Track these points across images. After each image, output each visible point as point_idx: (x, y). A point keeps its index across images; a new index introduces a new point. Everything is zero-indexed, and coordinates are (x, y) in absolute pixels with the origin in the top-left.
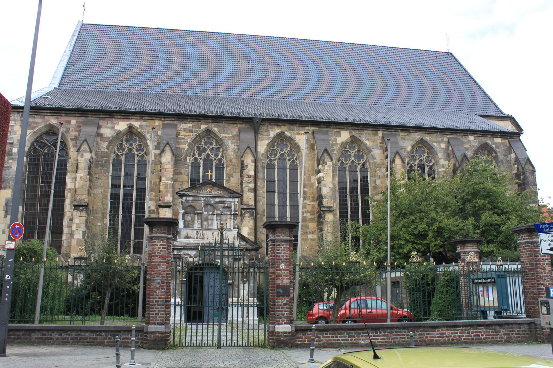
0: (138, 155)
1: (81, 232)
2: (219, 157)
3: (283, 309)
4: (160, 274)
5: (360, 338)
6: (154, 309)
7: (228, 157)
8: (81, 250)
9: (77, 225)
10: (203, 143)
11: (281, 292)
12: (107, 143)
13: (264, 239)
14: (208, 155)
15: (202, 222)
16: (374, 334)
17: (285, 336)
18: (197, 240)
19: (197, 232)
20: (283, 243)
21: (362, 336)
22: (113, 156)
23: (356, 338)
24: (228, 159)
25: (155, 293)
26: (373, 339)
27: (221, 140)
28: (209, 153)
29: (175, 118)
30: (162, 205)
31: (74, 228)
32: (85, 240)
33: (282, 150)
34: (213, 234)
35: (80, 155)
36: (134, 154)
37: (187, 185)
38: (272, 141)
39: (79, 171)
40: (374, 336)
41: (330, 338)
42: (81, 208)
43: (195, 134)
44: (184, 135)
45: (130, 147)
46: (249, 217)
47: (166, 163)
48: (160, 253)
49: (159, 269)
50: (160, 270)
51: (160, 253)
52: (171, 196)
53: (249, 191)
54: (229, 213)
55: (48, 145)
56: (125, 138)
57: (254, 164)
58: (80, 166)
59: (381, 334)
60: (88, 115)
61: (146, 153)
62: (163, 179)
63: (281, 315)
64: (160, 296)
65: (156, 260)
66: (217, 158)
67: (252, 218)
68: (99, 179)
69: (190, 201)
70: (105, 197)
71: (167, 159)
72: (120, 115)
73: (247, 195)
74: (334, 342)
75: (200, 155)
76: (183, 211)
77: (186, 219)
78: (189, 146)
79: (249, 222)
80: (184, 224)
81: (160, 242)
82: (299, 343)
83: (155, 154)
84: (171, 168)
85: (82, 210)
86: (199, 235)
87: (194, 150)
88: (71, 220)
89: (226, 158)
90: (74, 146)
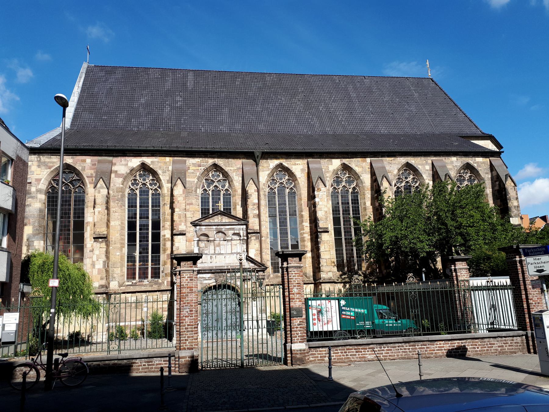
0: (152, 189)
1: (101, 263)
2: (226, 188)
3: (298, 329)
4: (188, 303)
5: (367, 353)
6: (184, 336)
8: (102, 279)
9: (97, 255)
10: (210, 175)
11: (295, 313)
12: (122, 179)
13: (268, 259)
14: (216, 186)
16: (379, 349)
17: (300, 354)
18: (211, 264)
19: (211, 257)
20: (294, 270)
21: (368, 351)
22: (127, 191)
23: (363, 353)
25: (184, 321)
26: (378, 354)
27: (226, 172)
28: (217, 185)
29: (184, 154)
31: (95, 259)
32: (106, 270)
33: (281, 179)
35: (97, 191)
36: (148, 188)
37: (198, 216)
38: (272, 171)
39: (97, 206)
40: (379, 351)
41: (340, 354)
42: (100, 240)
43: (203, 168)
45: (143, 182)
47: (179, 195)
48: (188, 285)
49: (187, 299)
50: (188, 300)
51: (188, 285)
53: (254, 217)
54: (238, 239)
55: (65, 183)
56: (138, 173)
57: (257, 193)
58: (97, 201)
59: (385, 349)
60: (102, 154)
63: (296, 335)
64: (189, 323)
65: (184, 291)
66: (224, 189)
67: (258, 240)
68: (116, 212)
69: (203, 230)
70: (122, 229)
72: (132, 153)
73: (252, 221)
74: (344, 357)
75: (208, 187)
76: (198, 239)
77: (200, 246)
78: (198, 179)
81: (188, 275)
82: (313, 359)
85: (102, 242)
86: (213, 259)
88: (92, 251)
90: (90, 183)
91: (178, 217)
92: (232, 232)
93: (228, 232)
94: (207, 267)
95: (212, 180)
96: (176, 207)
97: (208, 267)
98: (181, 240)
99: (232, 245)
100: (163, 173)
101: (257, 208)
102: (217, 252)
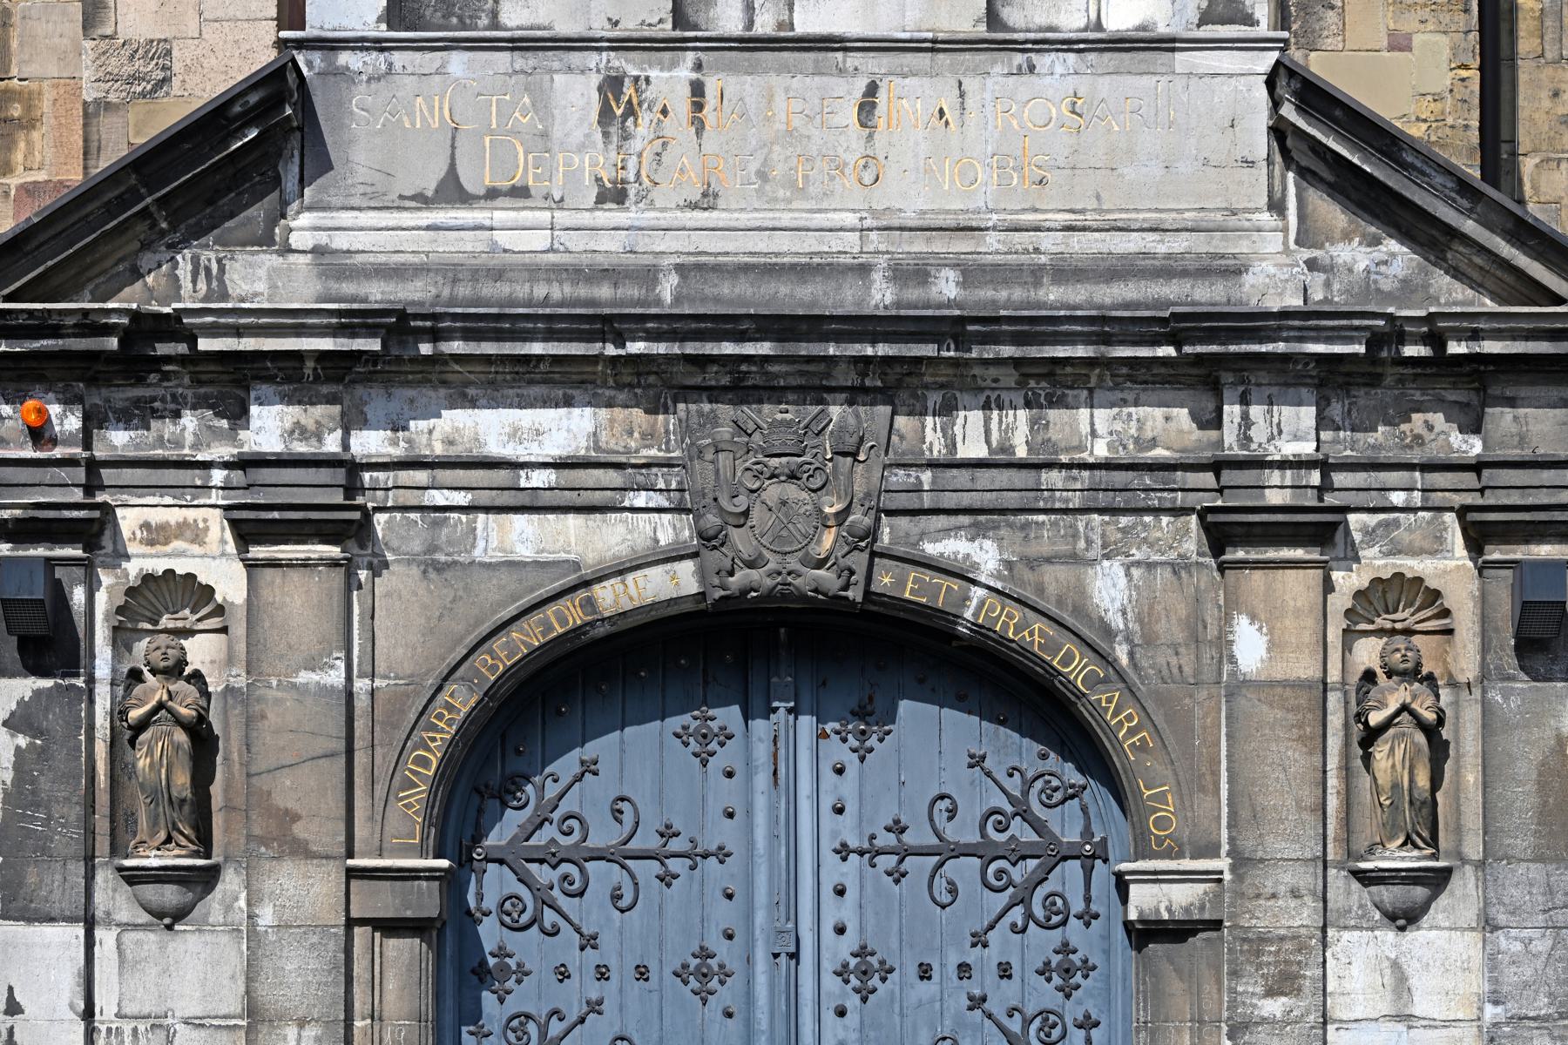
18: (610, 216)
19: (612, 85)
34: (867, 108)
86: (643, 128)
94: (534, 272)
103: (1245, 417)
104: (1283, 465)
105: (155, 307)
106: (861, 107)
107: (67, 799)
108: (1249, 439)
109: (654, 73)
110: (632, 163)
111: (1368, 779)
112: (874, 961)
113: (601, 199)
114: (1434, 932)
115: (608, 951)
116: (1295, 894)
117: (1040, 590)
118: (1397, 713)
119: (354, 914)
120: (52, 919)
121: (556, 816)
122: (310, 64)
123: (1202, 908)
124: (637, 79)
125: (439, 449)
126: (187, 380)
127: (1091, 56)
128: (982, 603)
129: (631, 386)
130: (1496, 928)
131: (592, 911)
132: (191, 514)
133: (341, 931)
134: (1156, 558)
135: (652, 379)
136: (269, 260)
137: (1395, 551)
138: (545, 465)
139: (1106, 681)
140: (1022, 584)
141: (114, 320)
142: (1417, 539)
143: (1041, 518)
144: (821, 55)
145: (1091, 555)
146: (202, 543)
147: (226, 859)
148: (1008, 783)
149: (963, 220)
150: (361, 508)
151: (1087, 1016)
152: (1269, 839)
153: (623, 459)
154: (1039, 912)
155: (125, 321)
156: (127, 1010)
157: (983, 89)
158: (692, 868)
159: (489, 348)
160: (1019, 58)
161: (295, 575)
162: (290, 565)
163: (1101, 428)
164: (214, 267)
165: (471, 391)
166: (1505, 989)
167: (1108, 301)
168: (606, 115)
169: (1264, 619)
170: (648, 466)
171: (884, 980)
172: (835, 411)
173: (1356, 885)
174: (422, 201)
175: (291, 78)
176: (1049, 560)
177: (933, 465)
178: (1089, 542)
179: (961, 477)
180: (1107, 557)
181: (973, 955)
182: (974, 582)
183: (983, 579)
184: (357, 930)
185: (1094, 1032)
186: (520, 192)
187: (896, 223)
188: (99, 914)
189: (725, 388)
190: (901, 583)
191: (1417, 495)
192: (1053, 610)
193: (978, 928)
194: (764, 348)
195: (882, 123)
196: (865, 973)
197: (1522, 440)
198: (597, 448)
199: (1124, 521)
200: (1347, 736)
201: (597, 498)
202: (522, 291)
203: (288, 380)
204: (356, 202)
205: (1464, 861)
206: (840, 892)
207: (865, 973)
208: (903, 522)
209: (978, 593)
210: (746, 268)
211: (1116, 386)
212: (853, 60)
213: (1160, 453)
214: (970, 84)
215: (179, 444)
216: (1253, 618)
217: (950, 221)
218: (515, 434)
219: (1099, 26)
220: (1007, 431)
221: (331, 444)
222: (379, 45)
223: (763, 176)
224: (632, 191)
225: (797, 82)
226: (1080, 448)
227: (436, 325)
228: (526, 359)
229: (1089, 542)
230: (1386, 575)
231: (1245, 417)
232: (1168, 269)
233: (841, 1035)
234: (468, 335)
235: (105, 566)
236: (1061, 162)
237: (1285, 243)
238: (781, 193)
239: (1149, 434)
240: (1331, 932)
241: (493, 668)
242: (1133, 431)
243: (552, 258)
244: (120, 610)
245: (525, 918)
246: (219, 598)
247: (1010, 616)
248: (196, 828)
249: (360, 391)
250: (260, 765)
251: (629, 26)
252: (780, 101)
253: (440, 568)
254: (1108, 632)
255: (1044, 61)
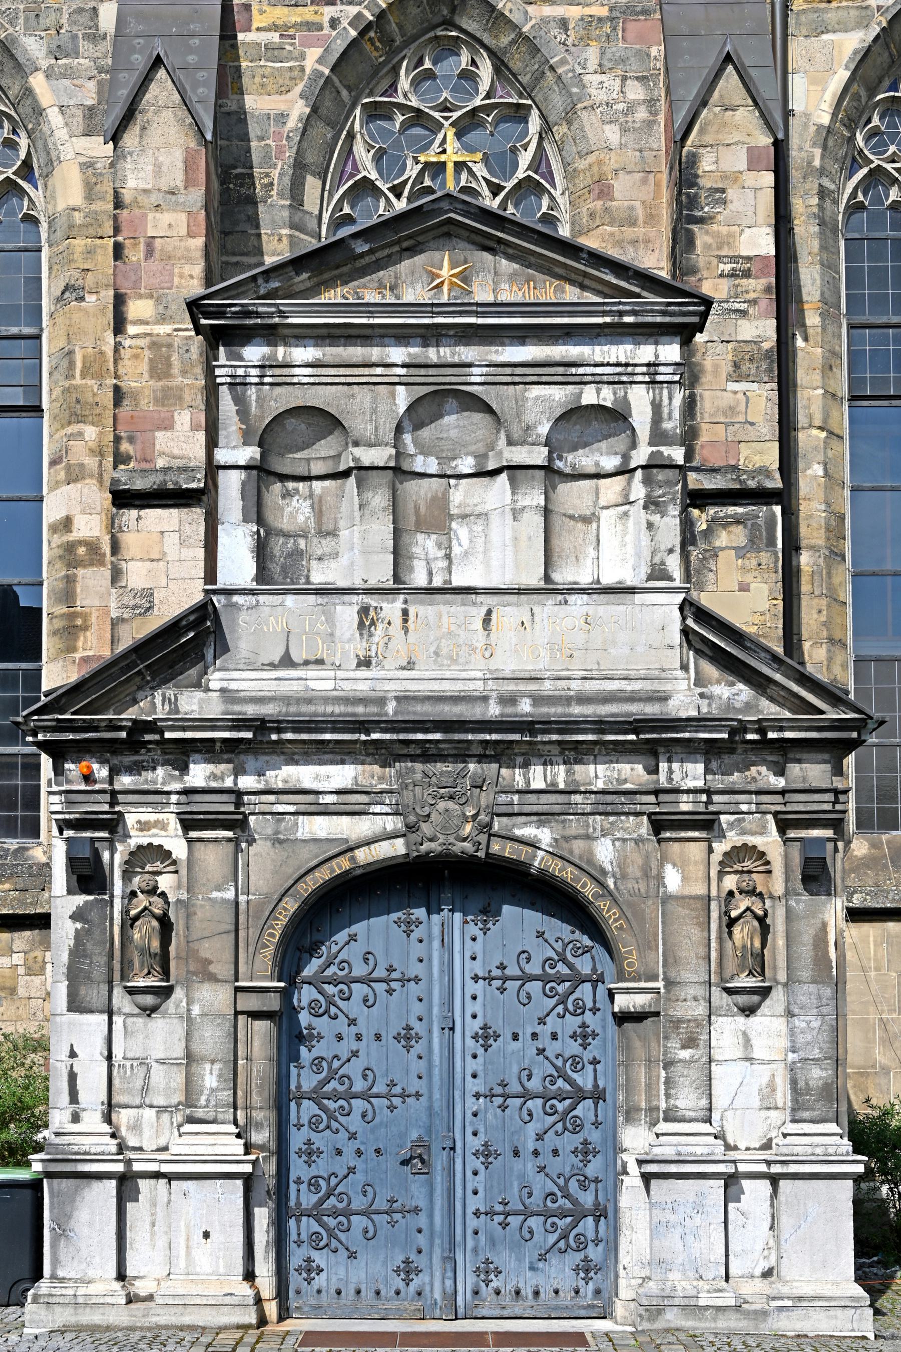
2: (520, 174)
7: (581, 164)
15: (397, 533)
18: (363, 673)
19: (364, 611)
24: (582, 181)
30: (139, 484)
34: (487, 621)
43: (353, 10)
44: (274, 27)
46: (741, 553)
47: (155, 198)
52: (194, 428)
53: (738, 373)
57: (769, 179)
61: (26, 171)
62: (137, 308)
66: (509, 185)
71: (158, 170)
73: (727, 399)
77: (270, 517)
79: (744, 588)
80: (261, 551)
83: (87, 166)
84: (191, 235)
86: (379, 631)
87: (351, 136)
89: (570, 175)
91: (144, 367)
92: (559, 395)
93: (520, 402)
94: (326, 700)
95: (418, 117)
96: (136, 284)
97: (337, 700)
98: (171, 542)
99: (557, 522)
100: (57, 53)
101: (767, 304)
102: (419, 579)
103: (670, 769)
104: (688, 792)
105: (144, 718)
106: (484, 621)
107: (100, 954)
108: (672, 779)
109: (384, 605)
110: (374, 648)
111: (730, 943)
112: (491, 1031)
113: (359, 665)
114: (764, 1018)
115: (362, 1027)
116: (695, 999)
117: (571, 852)
118: (745, 911)
119: (239, 1009)
120: (92, 1012)
121: (337, 961)
122: (219, 601)
123: (650, 1006)
124: (376, 608)
125: (280, 785)
126: (159, 752)
127: (595, 596)
128: (543, 858)
129: (373, 754)
130: (793, 1016)
131: (354, 1007)
132: (161, 816)
133: (232, 1017)
134: (627, 836)
135: (383, 751)
136: (199, 695)
137: (743, 833)
138: (332, 793)
139: (603, 896)
140: (562, 849)
141: (124, 723)
142: (754, 827)
143: (571, 817)
144: (465, 596)
145: (595, 835)
146: (166, 830)
147: (177, 982)
148: (555, 945)
149: (533, 674)
150: (243, 813)
151: (595, 1058)
152: (683, 973)
153: (369, 789)
154: (571, 1007)
155: (130, 724)
156: (129, 1055)
157: (543, 612)
158: (403, 986)
159: (304, 736)
160: (560, 597)
161: (211, 846)
162: (208, 840)
163: (600, 774)
164: (173, 698)
165: (296, 757)
166: (798, 1045)
167: (603, 713)
168: (361, 625)
169: (681, 865)
170: (381, 793)
171: (495, 1040)
172: (472, 766)
173: (725, 995)
174: (273, 666)
175: (210, 608)
176: (575, 838)
177: (519, 792)
178: (595, 829)
179: (532, 798)
180: (603, 836)
181: (539, 1029)
182: (539, 848)
183: (543, 847)
184: (240, 1017)
185: (598, 1066)
186: (320, 662)
187: (501, 676)
188: (115, 1009)
189: (418, 756)
190: (504, 849)
191: (753, 806)
192: (577, 861)
193: (541, 1016)
194: (437, 736)
195: (494, 628)
196: (486, 1038)
197: (804, 779)
198: (357, 784)
199: (611, 819)
200: (720, 923)
201: (357, 808)
202: (320, 709)
203: (208, 752)
204: (241, 667)
205: (778, 983)
206: (474, 998)
207: (486, 1038)
208: (504, 820)
209: (540, 854)
210: (428, 698)
211: (607, 754)
212: (480, 598)
213: (629, 786)
214: (536, 610)
215: (155, 783)
216: (674, 865)
217: (527, 675)
218: (317, 778)
219: (598, 582)
220: (555, 776)
221: (229, 783)
222: (252, 592)
223: (437, 654)
224: (374, 661)
225: (453, 609)
226: (590, 784)
227: (279, 726)
228: (323, 742)
229: (595, 829)
230: (739, 844)
231: (670, 769)
232: (632, 698)
233: (475, 1067)
234: (295, 730)
235: (119, 841)
236: (581, 647)
237: (689, 685)
238: (445, 662)
239: (623, 777)
240: (713, 1018)
241: (306, 890)
242: (616, 776)
243: (335, 693)
244: (126, 863)
245: (321, 1011)
246: (174, 856)
247: (556, 865)
248: (162, 967)
249: (243, 757)
250: (194, 936)
251: (372, 583)
252: (445, 619)
253: (281, 842)
254: (604, 872)
255: (572, 599)
